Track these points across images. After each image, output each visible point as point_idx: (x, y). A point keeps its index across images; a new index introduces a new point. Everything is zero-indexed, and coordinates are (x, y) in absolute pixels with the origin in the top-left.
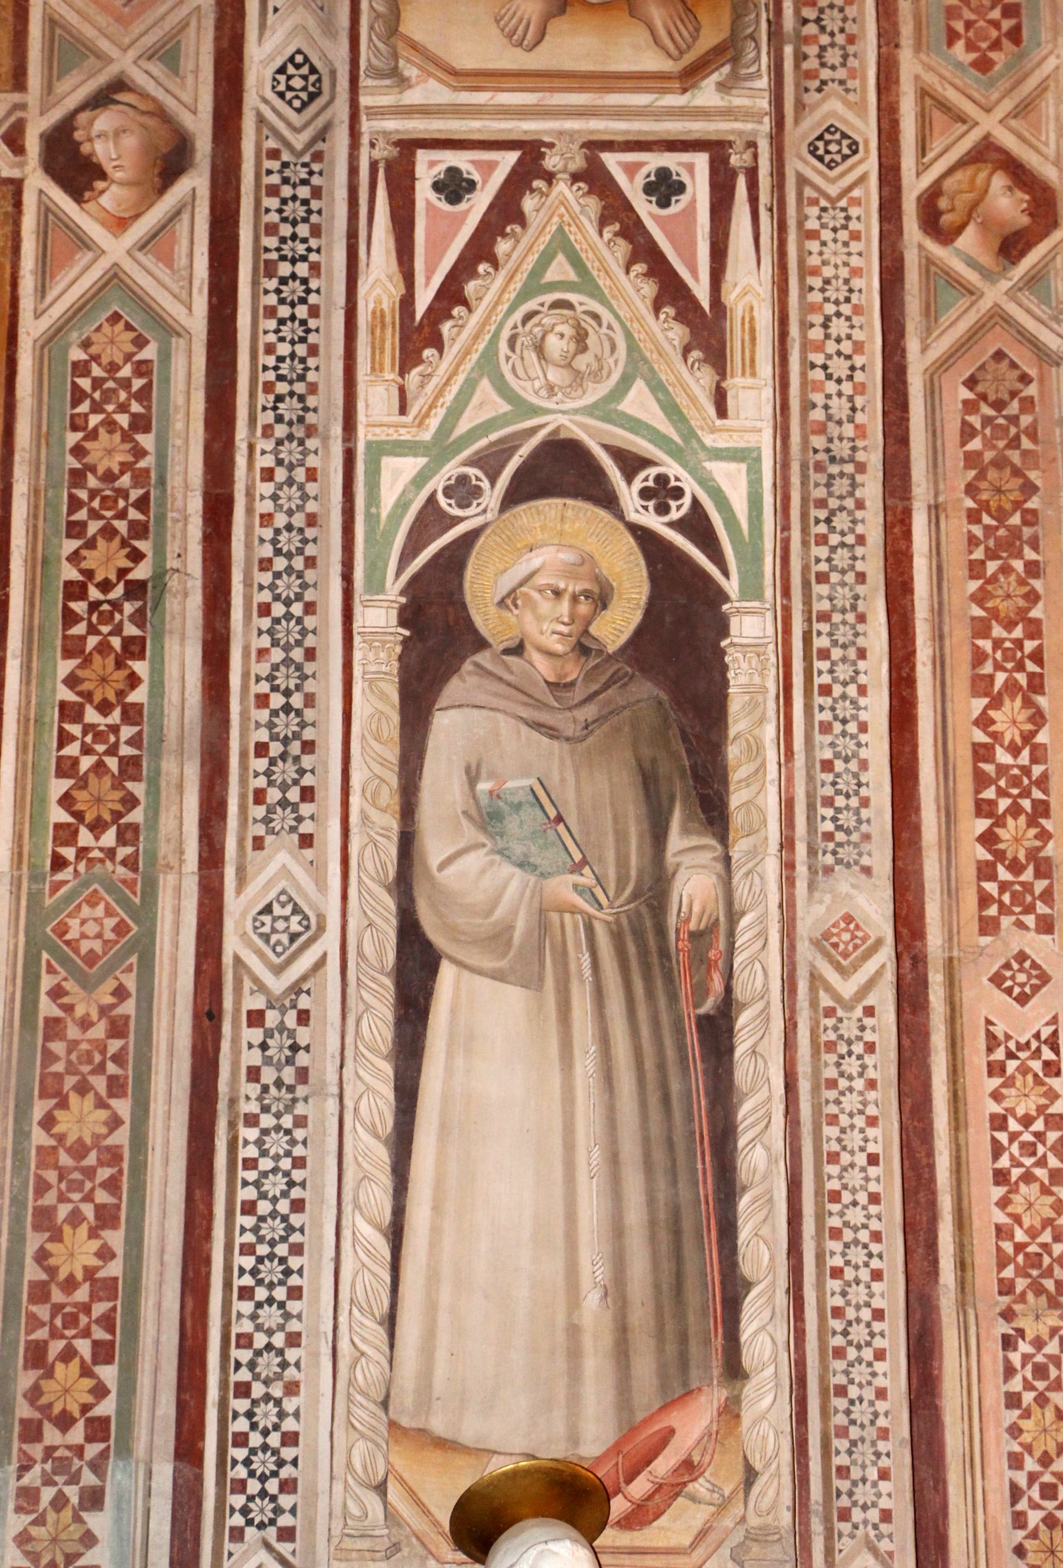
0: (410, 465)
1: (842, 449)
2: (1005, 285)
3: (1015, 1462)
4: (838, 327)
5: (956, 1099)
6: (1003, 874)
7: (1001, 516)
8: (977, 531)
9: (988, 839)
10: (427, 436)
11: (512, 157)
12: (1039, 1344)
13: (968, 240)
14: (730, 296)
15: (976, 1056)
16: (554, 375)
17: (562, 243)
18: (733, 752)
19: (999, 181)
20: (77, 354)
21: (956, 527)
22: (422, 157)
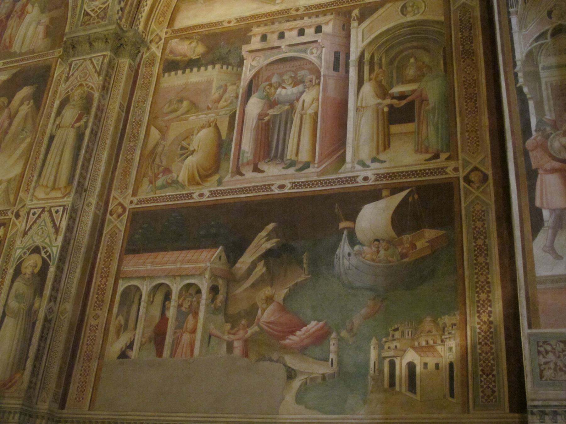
0: (20, 250)
1: (80, 245)
2: (117, 221)
3: (79, 383)
4: (84, 228)
5: (85, 334)
6: (98, 302)
7: (109, 253)
8: (106, 255)
9: (97, 298)
10: (23, 247)
11: (41, 209)
12: (86, 367)
13: (114, 216)
14: (61, 226)
15: (88, 328)
16: (39, 237)
17: (44, 220)
18: (46, 286)
19: (120, 207)
20: (12, 239)
21: (104, 254)
22: (32, 210)
